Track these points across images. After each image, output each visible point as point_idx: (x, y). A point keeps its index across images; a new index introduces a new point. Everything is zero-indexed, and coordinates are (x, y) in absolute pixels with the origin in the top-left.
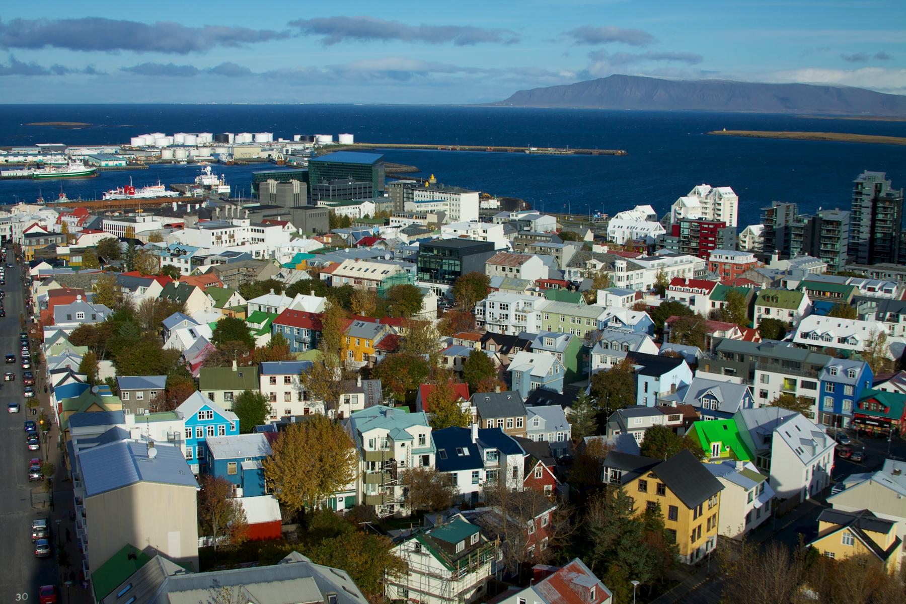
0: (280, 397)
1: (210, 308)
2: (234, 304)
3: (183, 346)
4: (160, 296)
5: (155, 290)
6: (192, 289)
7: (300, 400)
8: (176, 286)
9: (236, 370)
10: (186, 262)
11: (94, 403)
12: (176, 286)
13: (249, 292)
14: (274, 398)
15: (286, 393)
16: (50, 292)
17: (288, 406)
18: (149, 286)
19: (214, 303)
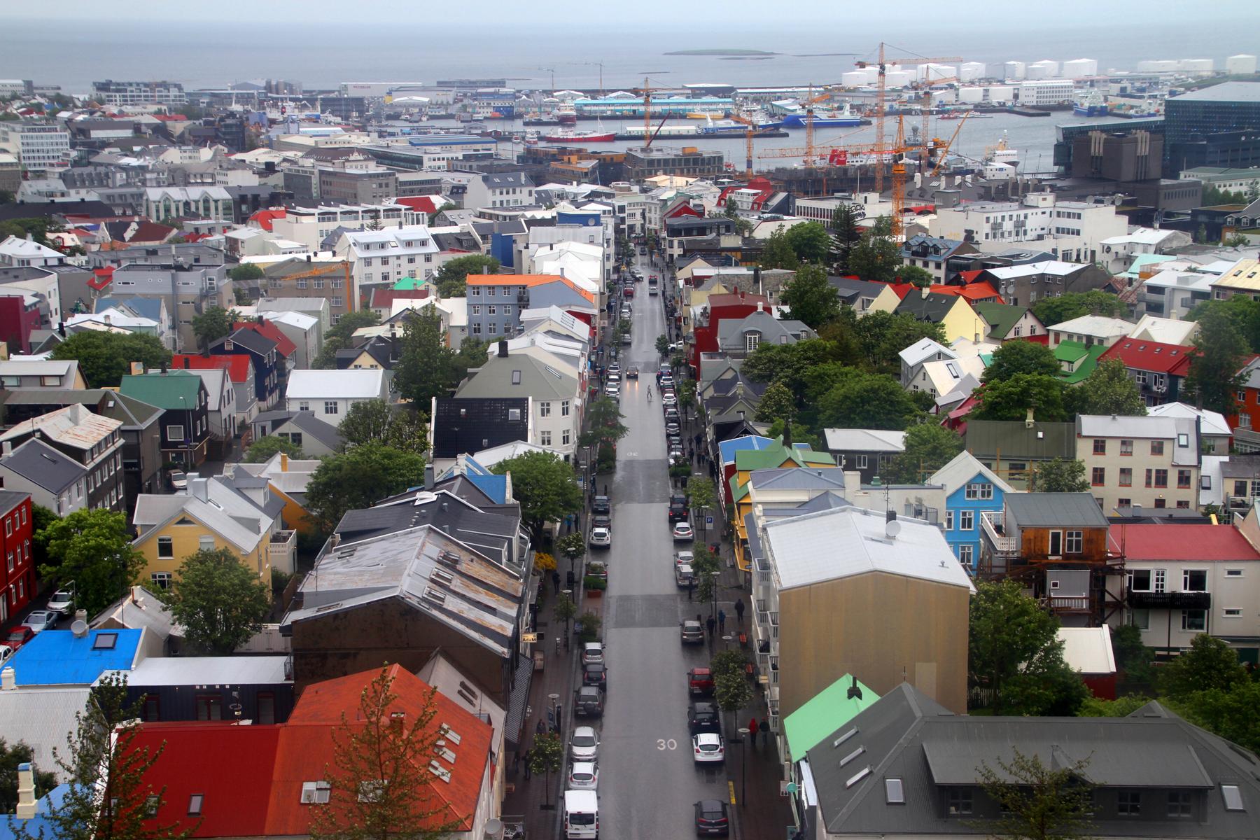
0: (1112, 477)
1: (981, 338)
2: (1026, 332)
3: (934, 390)
4: (896, 312)
5: (887, 300)
6: (951, 302)
7: (1148, 484)
8: (924, 296)
9: (1031, 426)
10: (938, 266)
11: (790, 459)
12: (924, 296)
13: (1051, 315)
14: (1099, 476)
15: (1123, 471)
16: (711, 297)
17: (1125, 493)
18: (876, 294)
19: (989, 330)
